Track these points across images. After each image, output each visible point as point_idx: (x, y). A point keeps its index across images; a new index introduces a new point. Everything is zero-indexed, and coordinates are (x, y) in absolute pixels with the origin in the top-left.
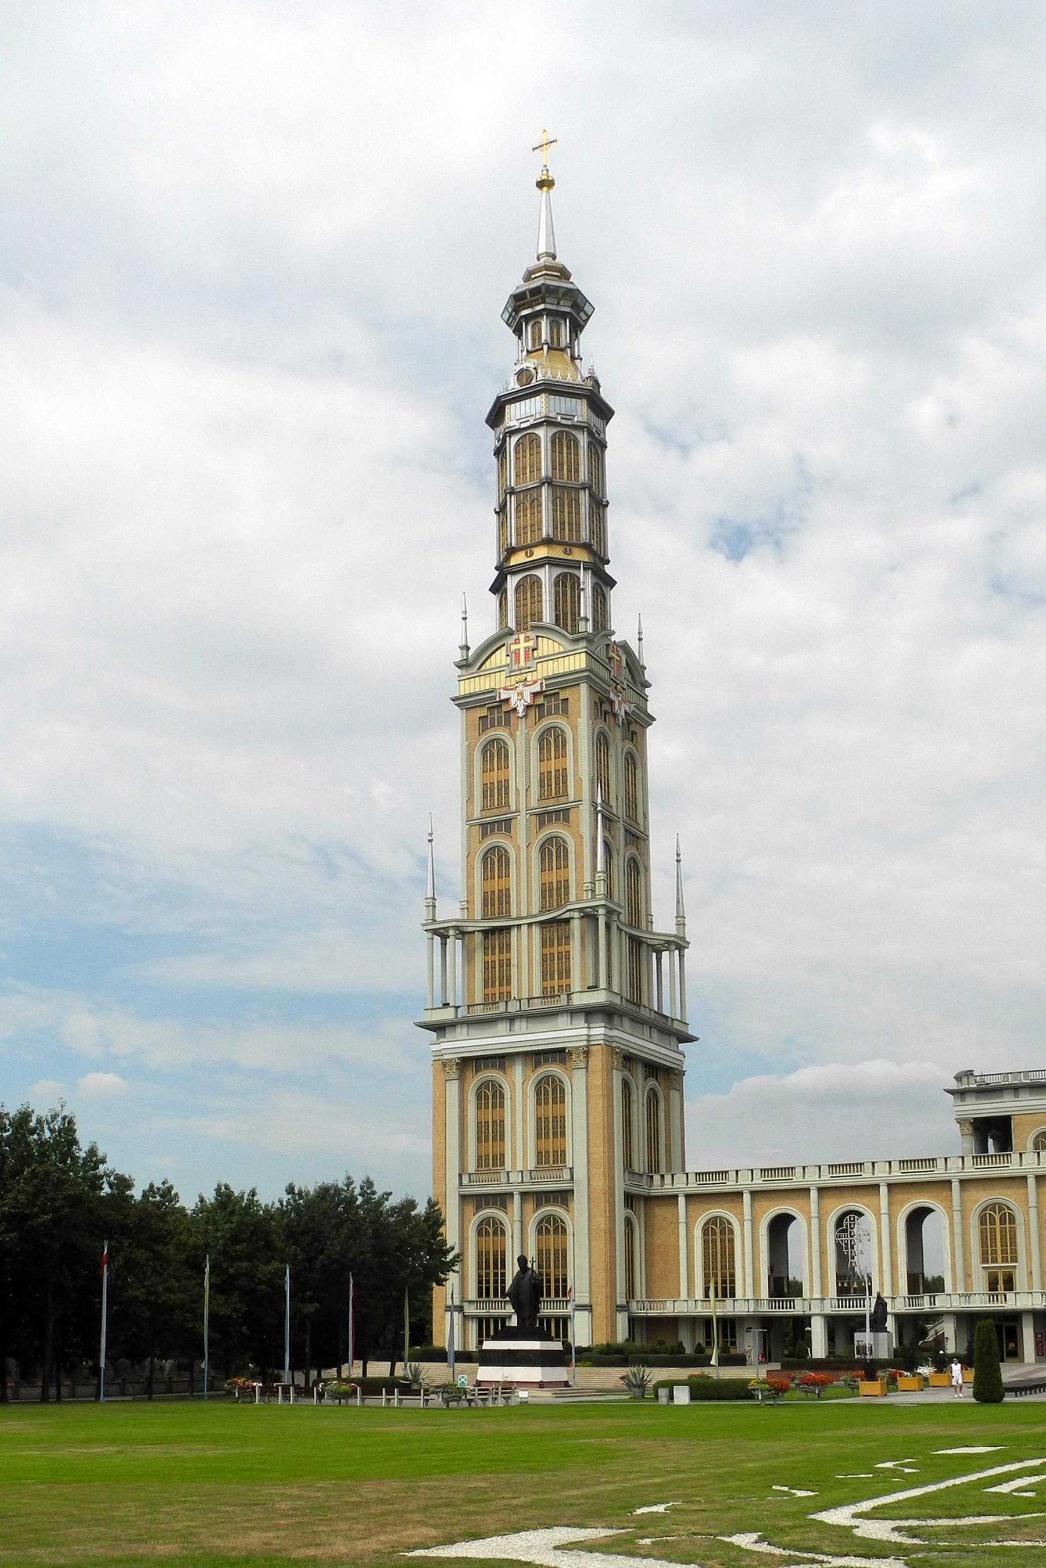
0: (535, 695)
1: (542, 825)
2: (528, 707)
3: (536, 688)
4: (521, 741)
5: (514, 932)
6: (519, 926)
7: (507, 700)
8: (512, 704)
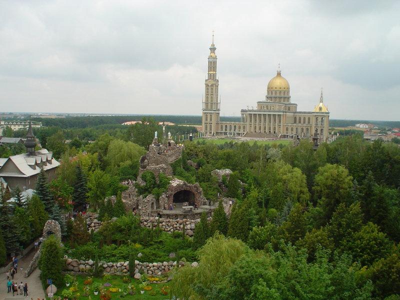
4: (210, 88)
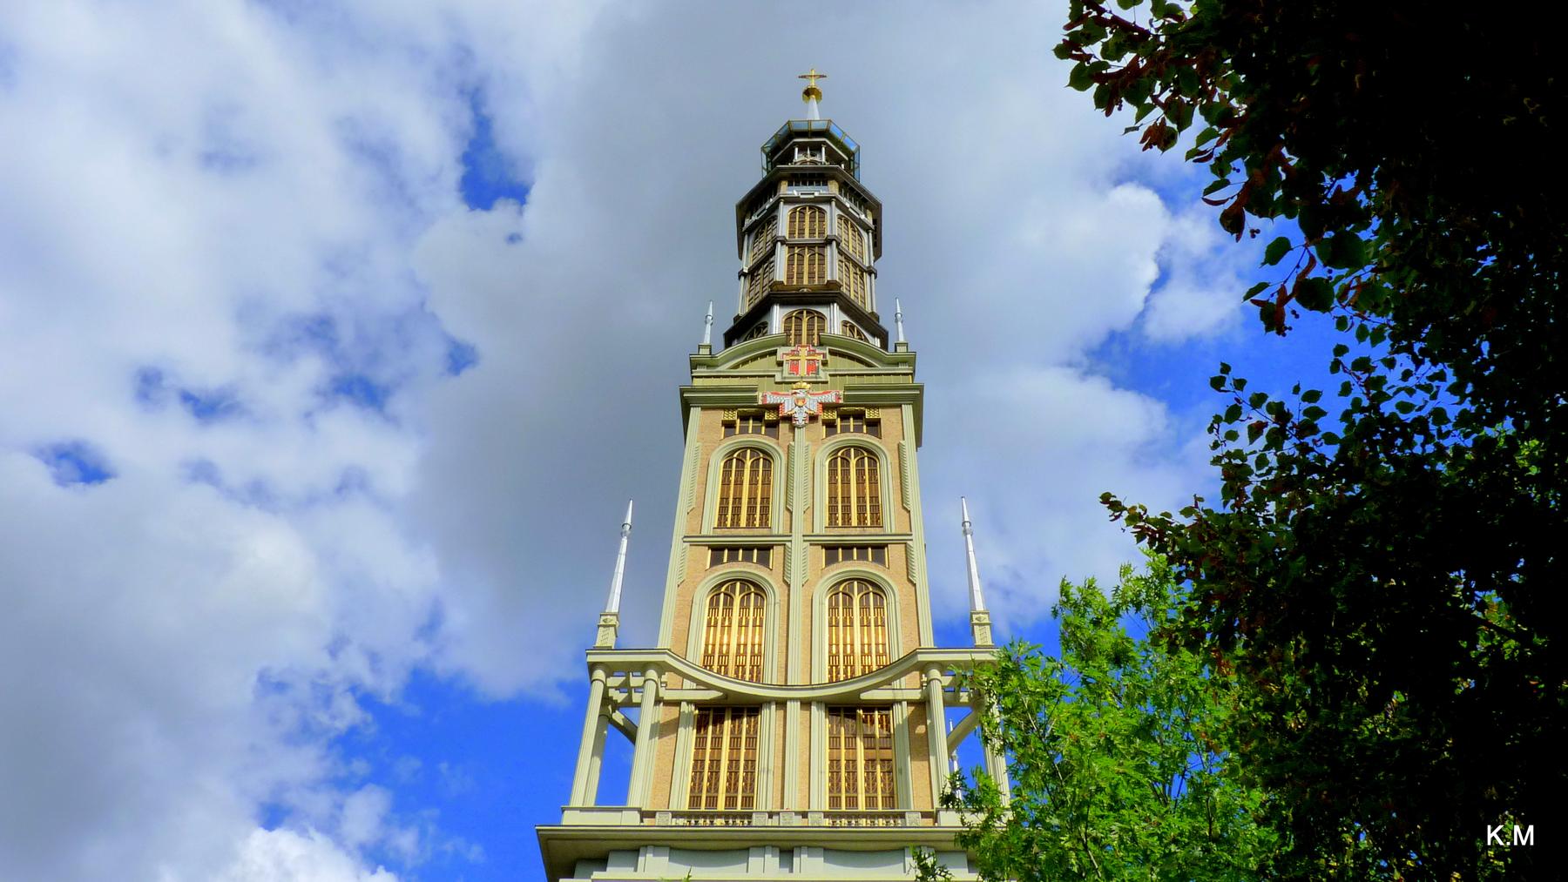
0: (827, 407)
1: (831, 560)
2: (813, 418)
3: (830, 398)
5: (769, 716)
6: (781, 704)
7: (775, 408)
8: (787, 410)
